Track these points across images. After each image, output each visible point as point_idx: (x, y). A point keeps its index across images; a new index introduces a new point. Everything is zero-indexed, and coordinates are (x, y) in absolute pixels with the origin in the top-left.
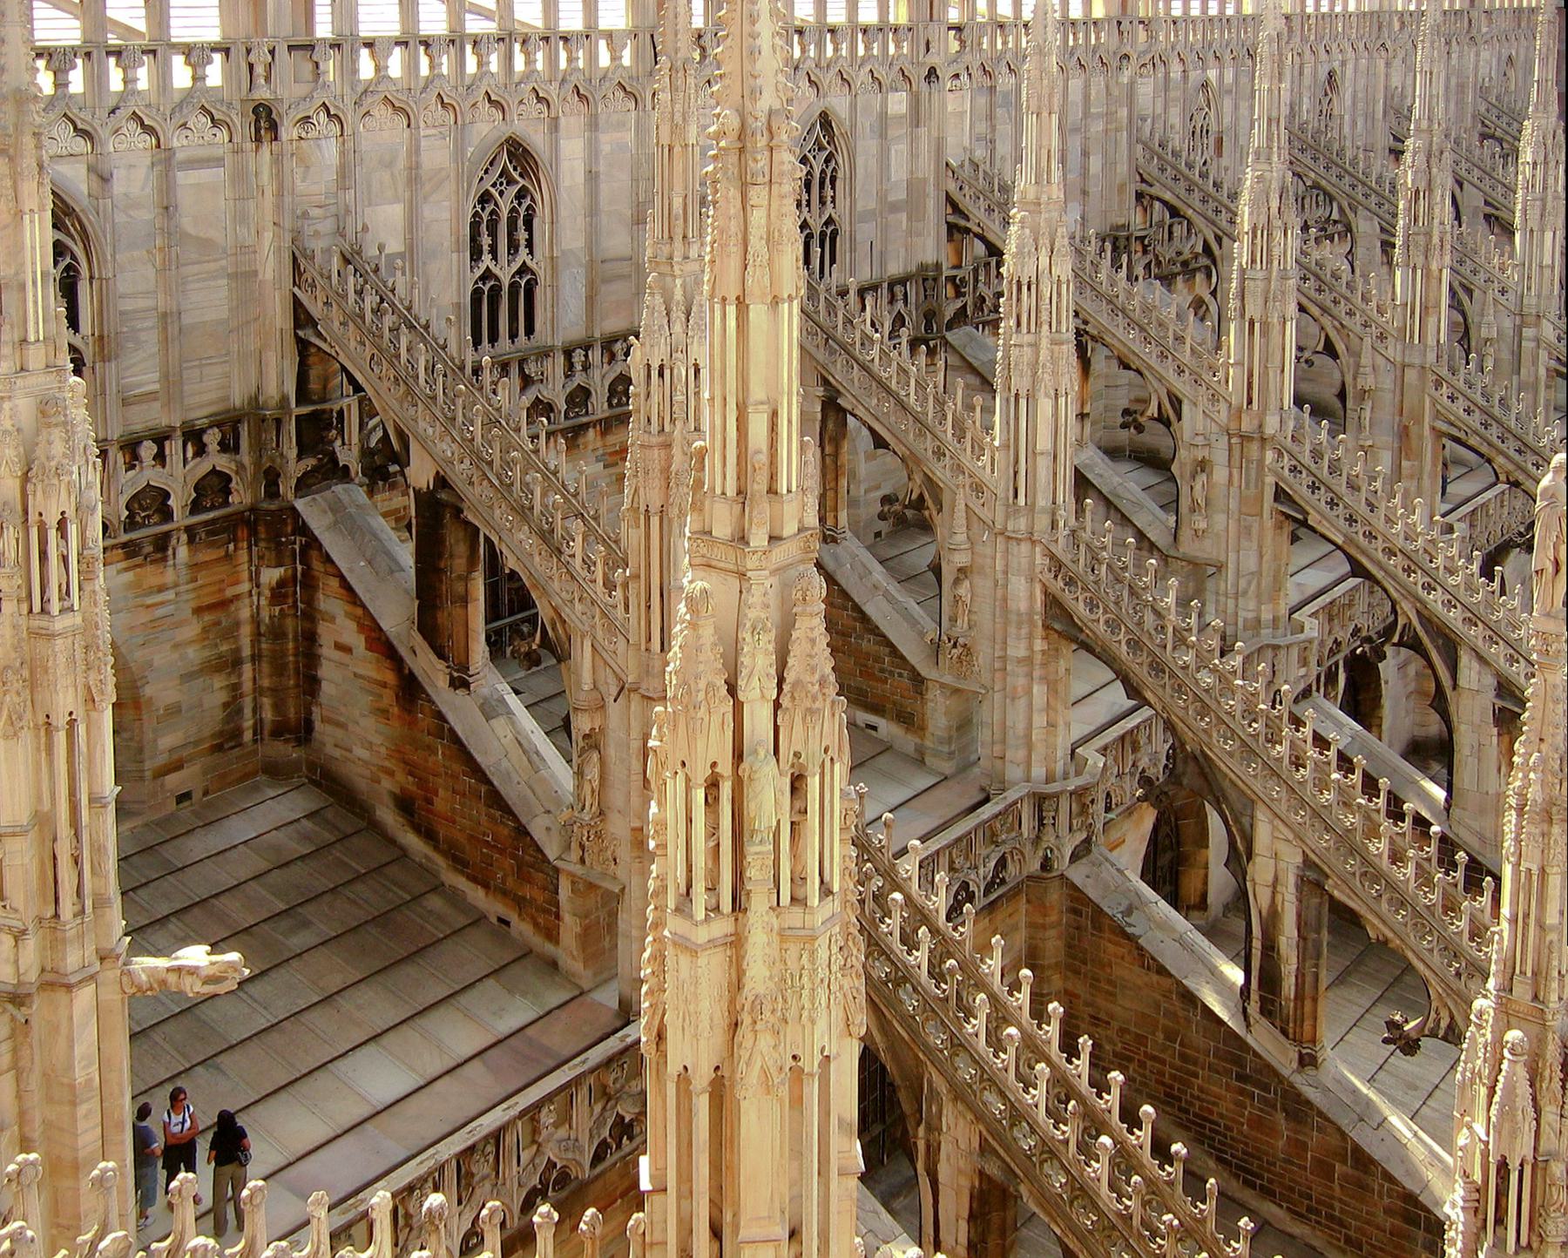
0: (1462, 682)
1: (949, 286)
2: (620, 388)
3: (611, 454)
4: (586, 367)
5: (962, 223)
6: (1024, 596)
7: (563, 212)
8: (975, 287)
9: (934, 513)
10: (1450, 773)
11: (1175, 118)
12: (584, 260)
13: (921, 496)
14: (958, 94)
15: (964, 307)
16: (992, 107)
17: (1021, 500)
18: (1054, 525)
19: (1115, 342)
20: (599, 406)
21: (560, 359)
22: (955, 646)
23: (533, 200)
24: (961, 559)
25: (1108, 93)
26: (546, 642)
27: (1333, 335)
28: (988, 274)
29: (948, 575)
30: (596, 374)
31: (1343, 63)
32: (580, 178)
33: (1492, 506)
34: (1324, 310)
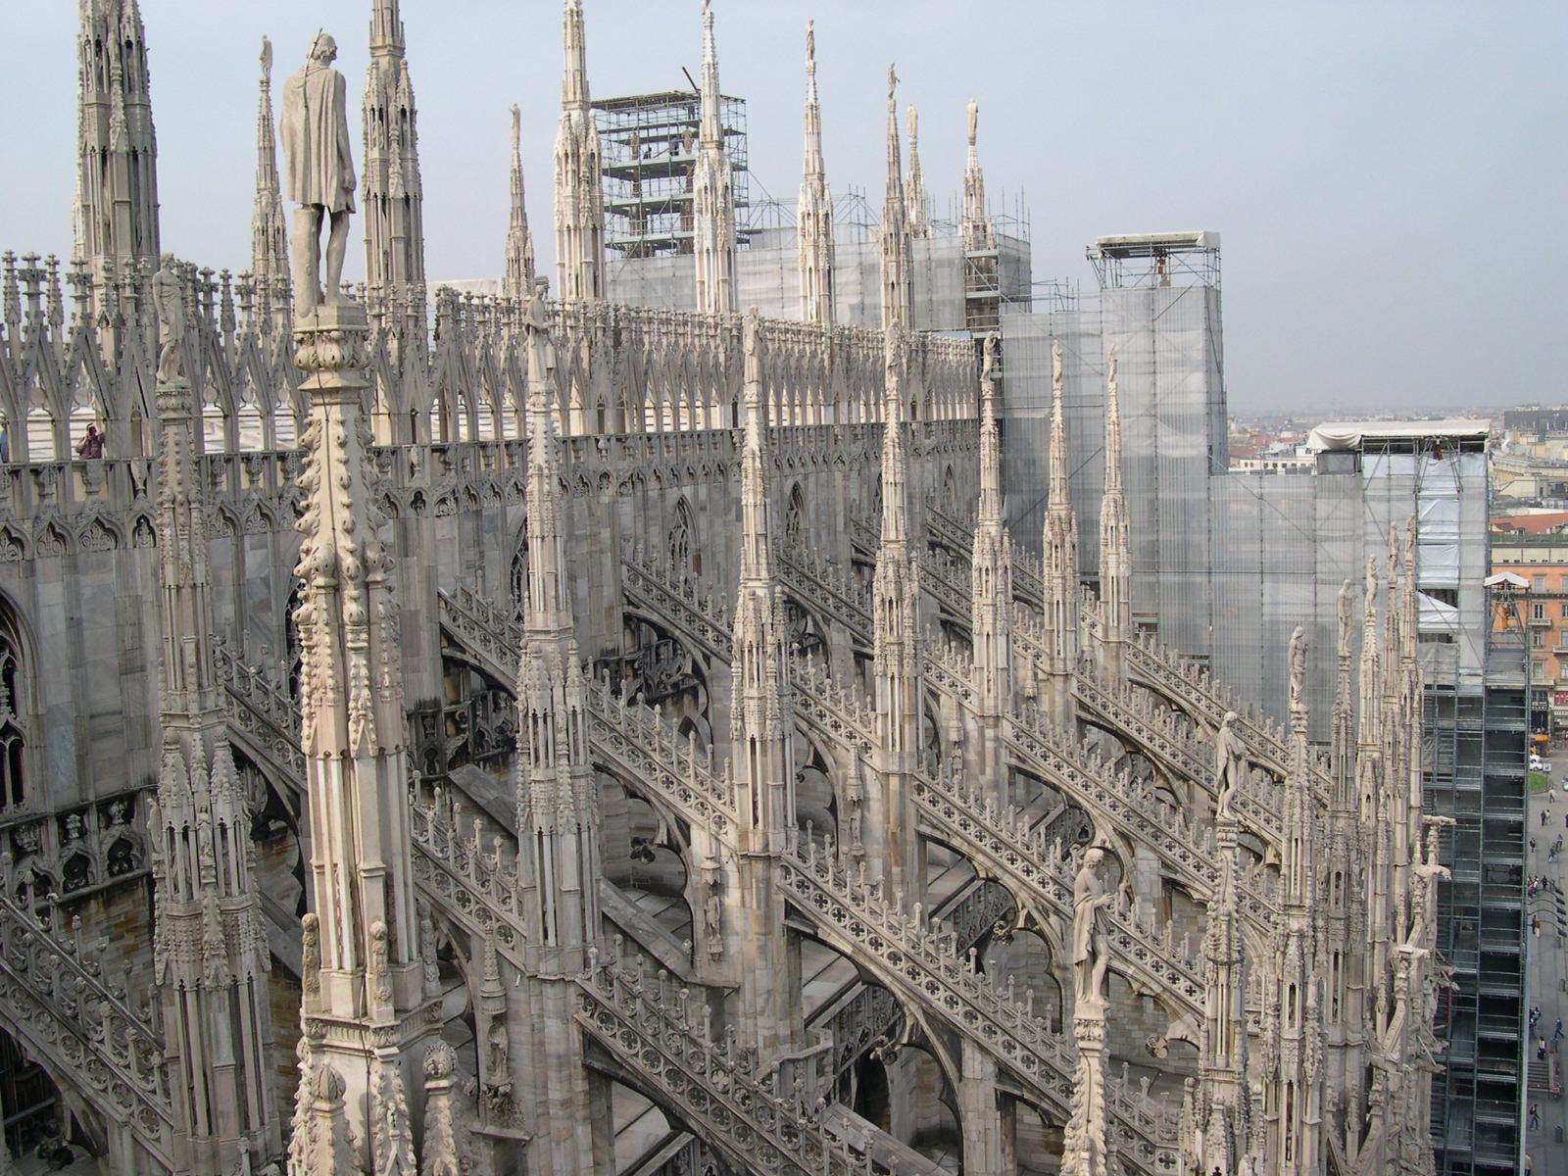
0: (967, 1073)
1: (449, 723)
2: (120, 854)
3: (116, 926)
4: (83, 833)
5: (459, 655)
6: (560, 1038)
7: (47, 665)
8: (475, 724)
9: (464, 961)
10: (961, 1159)
11: (656, 536)
12: (72, 715)
13: (448, 945)
14: (446, 520)
15: (465, 744)
16: (479, 531)
17: (551, 941)
18: (586, 963)
19: (621, 771)
20: (100, 876)
21: (53, 827)
22: (495, 1095)
23: (12, 652)
24: (494, 1008)
25: (591, 515)
26: (78, 1137)
27: (821, 748)
28: (485, 708)
29: (483, 1025)
30: (93, 841)
31: (806, 477)
32: (61, 626)
33: (970, 903)
34: (811, 724)
